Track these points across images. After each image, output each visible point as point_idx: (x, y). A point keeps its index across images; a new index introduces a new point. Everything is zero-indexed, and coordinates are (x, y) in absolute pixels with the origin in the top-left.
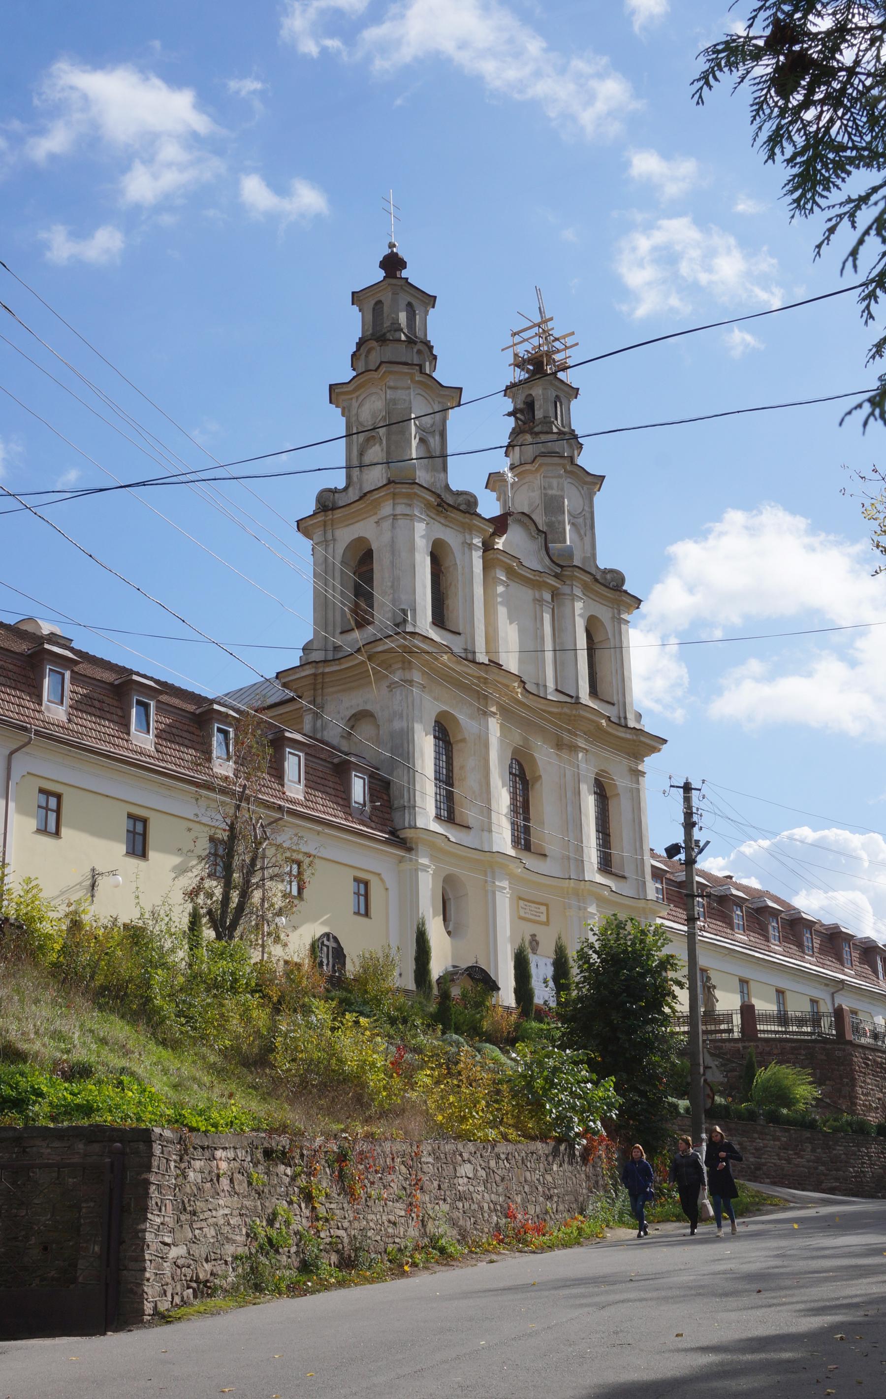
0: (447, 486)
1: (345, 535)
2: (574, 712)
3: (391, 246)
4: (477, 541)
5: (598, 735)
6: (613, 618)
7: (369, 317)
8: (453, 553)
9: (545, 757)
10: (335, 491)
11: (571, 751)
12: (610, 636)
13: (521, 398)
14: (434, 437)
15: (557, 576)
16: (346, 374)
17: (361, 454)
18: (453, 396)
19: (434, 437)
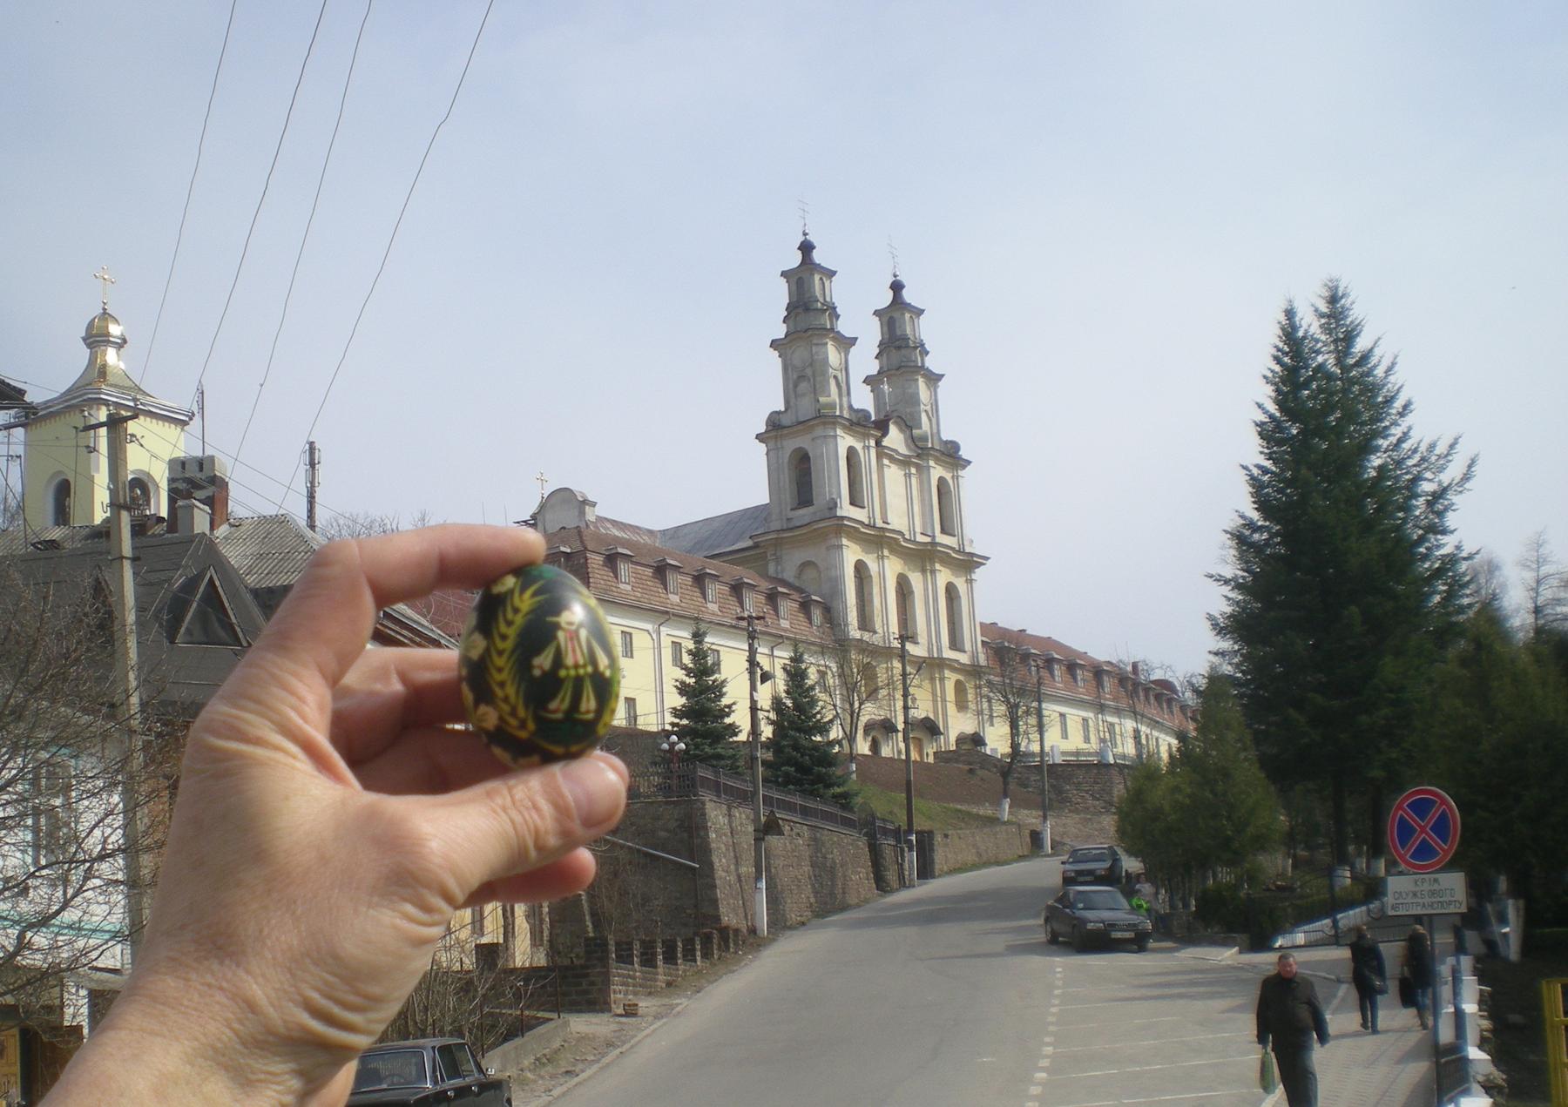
0: (850, 407)
1: (791, 444)
3: (805, 234)
4: (873, 443)
5: (948, 561)
7: (794, 288)
9: (916, 579)
10: (779, 413)
13: (885, 319)
15: (918, 456)
16: (780, 331)
17: (796, 386)
18: (853, 341)
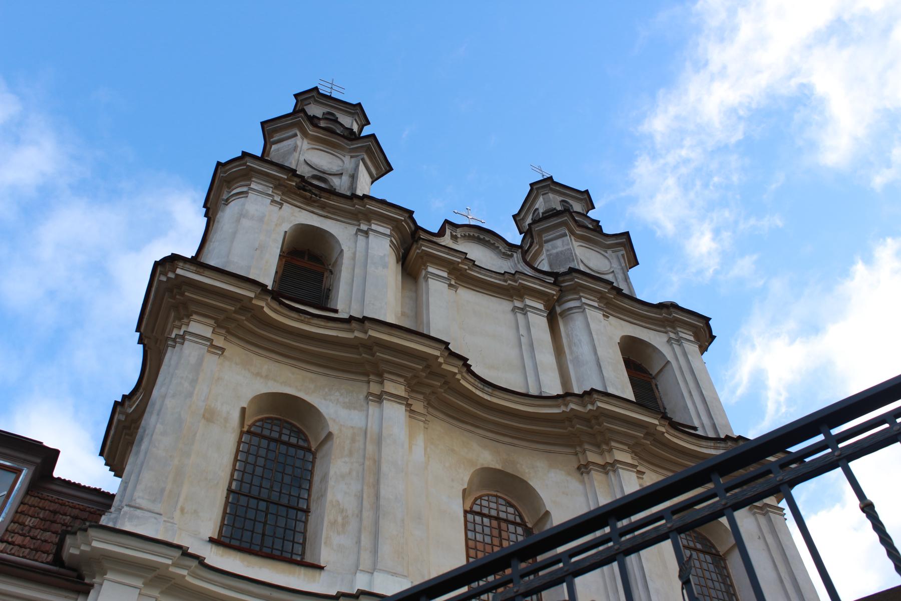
2: (590, 407)
6: (670, 339)
8: (337, 242)
11: (607, 473)
12: (669, 357)
14: (341, 178)
19: (341, 178)
